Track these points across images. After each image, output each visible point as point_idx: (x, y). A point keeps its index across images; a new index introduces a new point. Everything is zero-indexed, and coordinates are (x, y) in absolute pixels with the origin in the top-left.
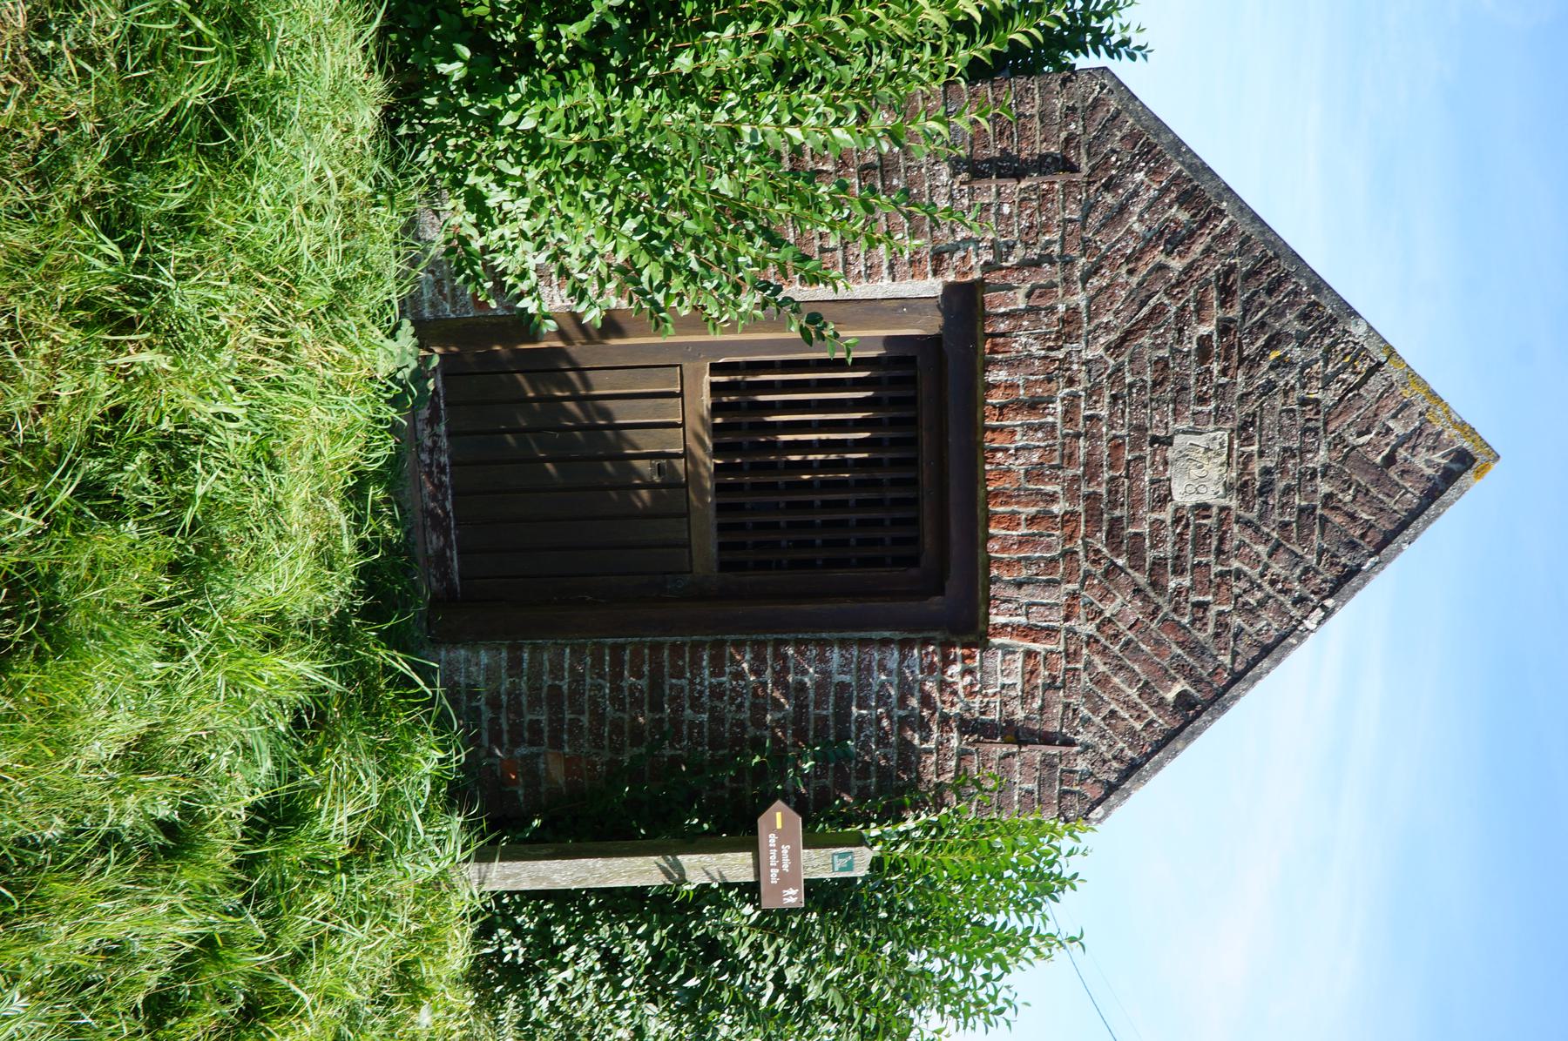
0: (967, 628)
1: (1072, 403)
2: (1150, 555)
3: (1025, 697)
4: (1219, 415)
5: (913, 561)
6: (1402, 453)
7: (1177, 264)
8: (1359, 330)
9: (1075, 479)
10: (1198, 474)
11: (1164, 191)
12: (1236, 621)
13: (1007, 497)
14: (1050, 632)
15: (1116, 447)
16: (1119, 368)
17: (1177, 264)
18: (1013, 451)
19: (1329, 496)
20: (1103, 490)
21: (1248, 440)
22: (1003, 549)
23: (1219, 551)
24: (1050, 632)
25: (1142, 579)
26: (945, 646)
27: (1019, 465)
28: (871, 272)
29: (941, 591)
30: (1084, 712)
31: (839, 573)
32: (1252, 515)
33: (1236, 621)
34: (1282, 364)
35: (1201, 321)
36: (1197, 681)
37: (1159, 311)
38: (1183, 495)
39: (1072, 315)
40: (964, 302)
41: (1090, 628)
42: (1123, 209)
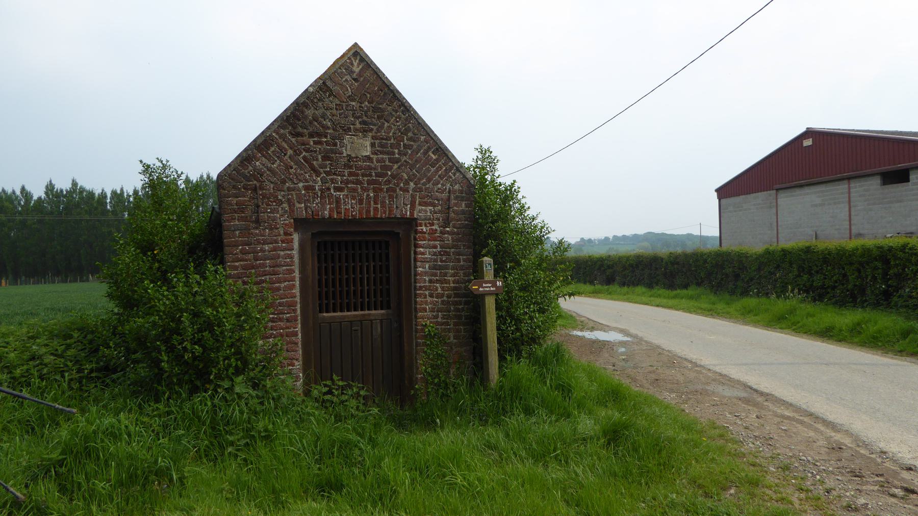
0: (411, 223)
1: (337, 189)
2: (387, 163)
3: (434, 205)
4: (341, 139)
5: (387, 243)
6: (355, 76)
7: (290, 152)
8: (311, 89)
9: (362, 188)
10: (363, 147)
11: (264, 156)
12: (410, 134)
13: (368, 211)
14: (413, 197)
15: (350, 174)
16: (325, 172)
17: (290, 152)
18: (351, 207)
19: (369, 102)
20: (366, 179)
21: (349, 129)
22: (385, 213)
23: (386, 139)
24: (413, 197)
25: (396, 166)
26: (416, 232)
27: (357, 207)
28: (291, 257)
29: (398, 233)
30: (440, 186)
31: (391, 269)
32: (375, 128)
33: (410, 134)
34: (324, 116)
35: (308, 144)
36: (429, 148)
37: (305, 158)
38: (367, 152)
39: (307, 188)
40: (300, 224)
41: (412, 184)
42: (270, 169)
